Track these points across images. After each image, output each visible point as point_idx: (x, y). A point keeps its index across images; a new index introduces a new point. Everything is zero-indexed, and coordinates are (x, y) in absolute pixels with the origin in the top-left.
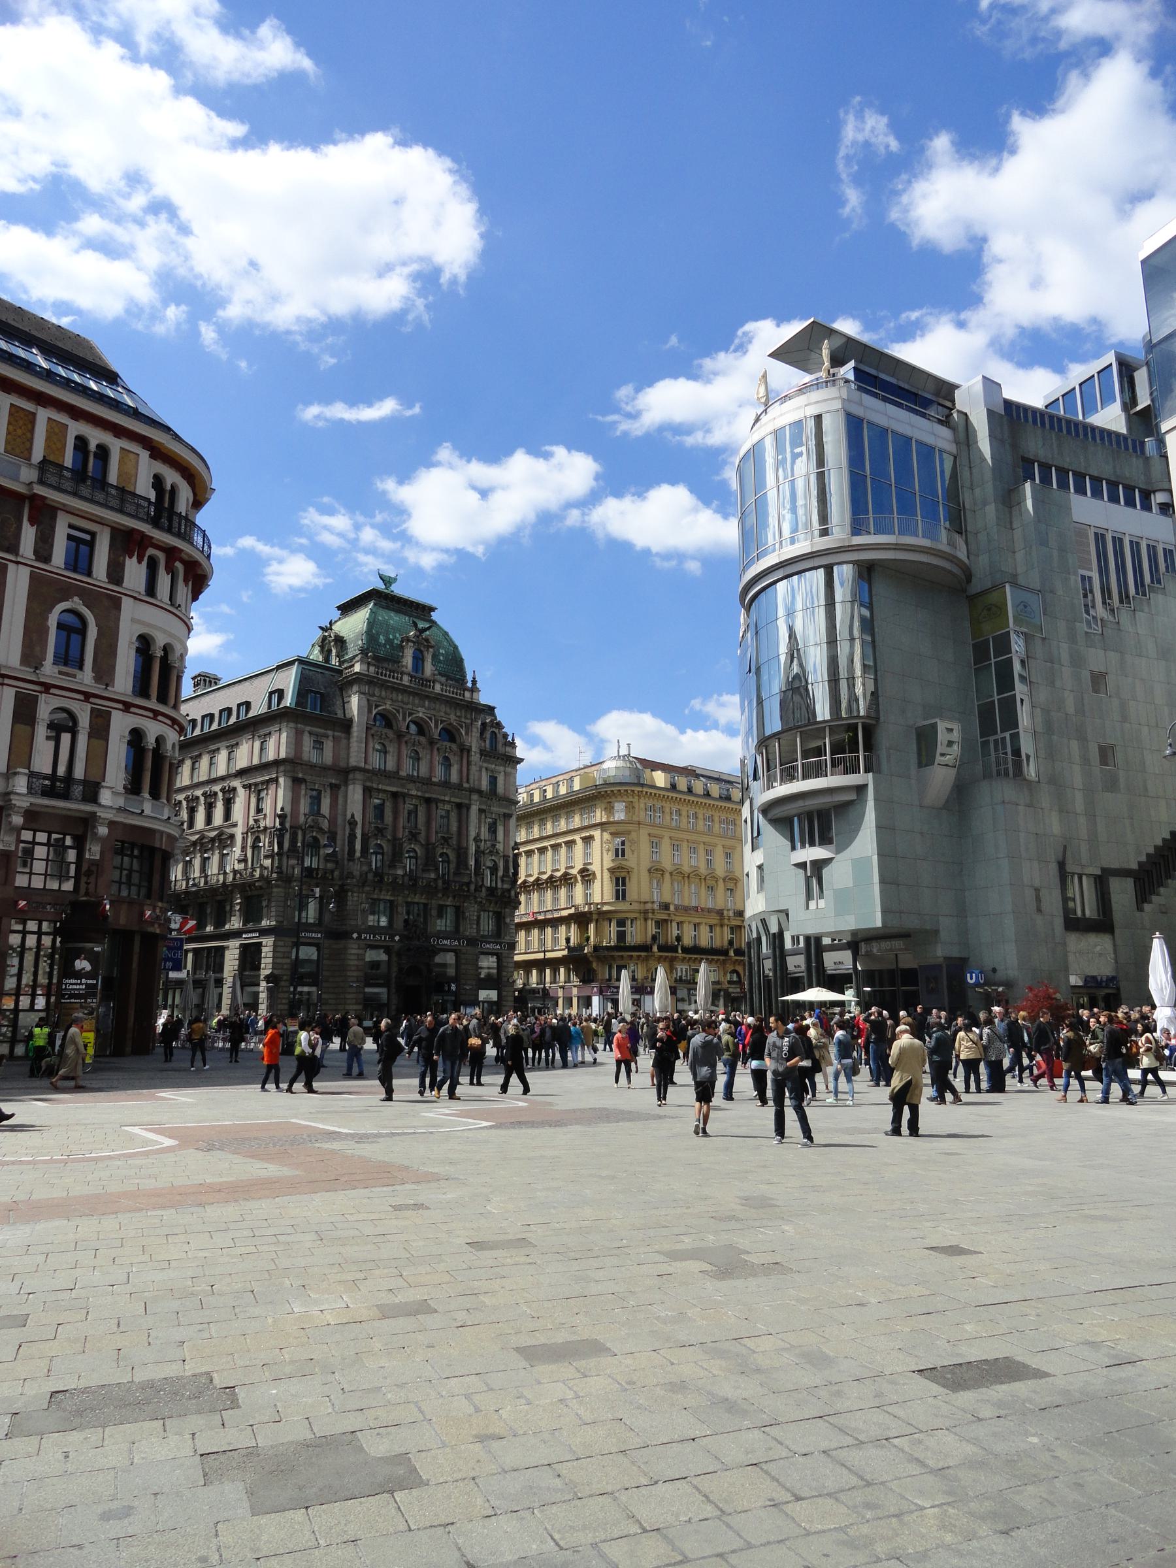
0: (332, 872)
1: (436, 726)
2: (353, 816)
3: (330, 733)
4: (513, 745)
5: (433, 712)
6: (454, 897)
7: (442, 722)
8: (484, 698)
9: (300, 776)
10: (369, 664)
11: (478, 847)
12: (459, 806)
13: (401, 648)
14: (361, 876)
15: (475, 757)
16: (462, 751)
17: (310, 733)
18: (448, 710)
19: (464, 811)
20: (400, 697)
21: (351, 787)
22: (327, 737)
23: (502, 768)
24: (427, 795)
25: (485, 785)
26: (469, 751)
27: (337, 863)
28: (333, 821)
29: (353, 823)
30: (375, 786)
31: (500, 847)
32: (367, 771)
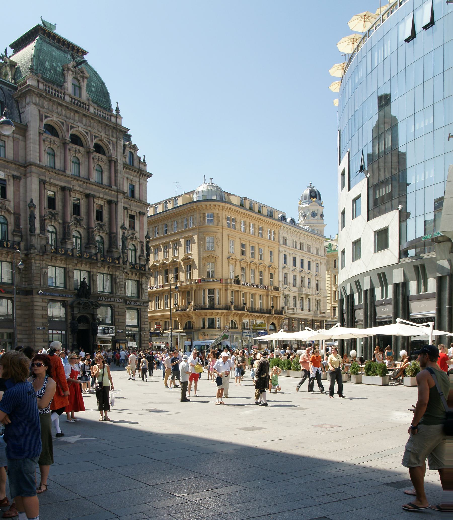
0: (19, 244)
1: (92, 140)
2: (32, 201)
4: (144, 163)
5: (89, 129)
6: (109, 268)
7: (96, 137)
8: (124, 123)
10: (38, 81)
11: (124, 233)
12: (110, 202)
13: (63, 74)
14: (41, 248)
15: (120, 168)
16: (110, 161)
18: (100, 129)
20: (64, 112)
21: (29, 179)
23: (137, 179)
24: (87, 192)
25: (126, 189)
26: (116, 162)
27: (21, 237)
28: (17, 206)
29: (31, 206)
30: (48, 179)
31: (137, 235)
32: (41, 167)
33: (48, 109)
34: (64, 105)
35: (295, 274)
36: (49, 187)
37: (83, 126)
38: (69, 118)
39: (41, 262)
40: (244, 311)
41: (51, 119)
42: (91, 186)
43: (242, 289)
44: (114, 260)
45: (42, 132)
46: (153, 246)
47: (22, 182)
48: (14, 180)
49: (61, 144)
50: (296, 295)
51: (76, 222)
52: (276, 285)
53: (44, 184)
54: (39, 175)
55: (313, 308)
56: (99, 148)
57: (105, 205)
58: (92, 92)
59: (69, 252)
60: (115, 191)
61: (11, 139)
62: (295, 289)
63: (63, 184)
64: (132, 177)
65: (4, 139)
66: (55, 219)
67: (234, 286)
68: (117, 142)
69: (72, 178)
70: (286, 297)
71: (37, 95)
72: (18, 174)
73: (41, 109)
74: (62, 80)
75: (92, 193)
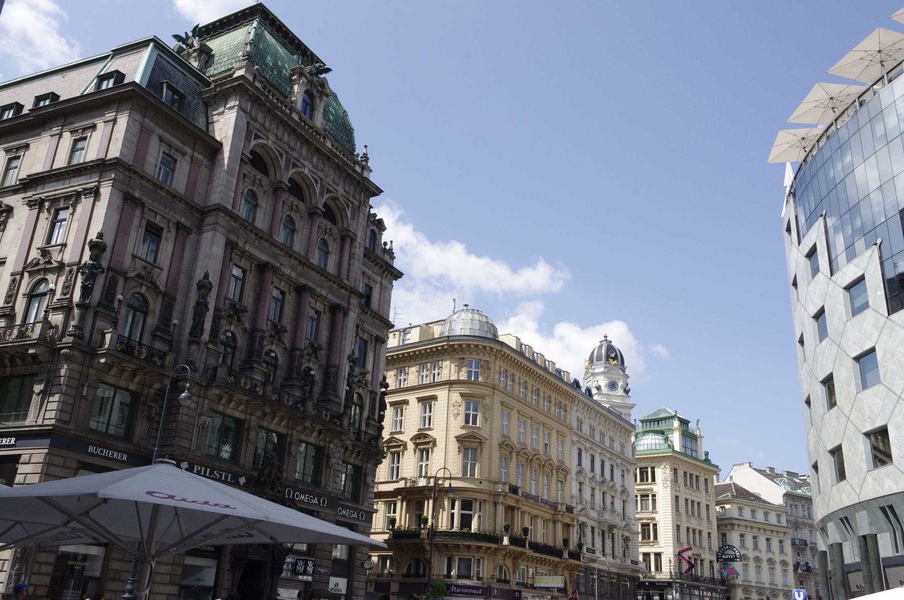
0: (162, 356)
1: (322, 194)
2: (206, 276)
3: (188, 150)
5: (320, 174)
6: (320, 432)
7: (328, 191)
9: (137, 194)
14: (206, 370)
16: (343, 238)
17: (161, 139)
19: (340, 315)
20: (286, 138)
21: (207, 236)
22: (184, 154)
24: (303, 281)
26: (353, 240)
28: (173, 282)
30: (241, 243)
33: (263, 125)
34: (290, 126)
35: (593, 485)
36: (237, 258)
37: (312, 168)
38: (293, 150)
39: (201, 400)
40: (524, 546)
41: (265, 142)
42: (310, 271)
43: (520, 506)
44: (333, 417)
45: (246, 160)
46: (392, 404)
47: (193, 236)
48: (177, 232)
49: (271, 190)
50: (595, 524)
51: (274, 333)
52: (567, 501)
53: (233, 248)
54: (229, 232)
55: (619, 551)
56: (329, 214)
57: (325, 312)
58: (329, 120)
59: (258, 389)
60: (347, 290)
61: (188, 158)
62: (594, 514)
63: (264, 258)
64: (370, 273)
65: (175, 156)
66: (239, 320)
67: (510, 497)
68: (359, 207)
69: (282, 250)
70: (582, 525)
71: (250, 96)
72: (188, 224)
73: (252, 122)
74: (289, 89)
75: (310, 284)
